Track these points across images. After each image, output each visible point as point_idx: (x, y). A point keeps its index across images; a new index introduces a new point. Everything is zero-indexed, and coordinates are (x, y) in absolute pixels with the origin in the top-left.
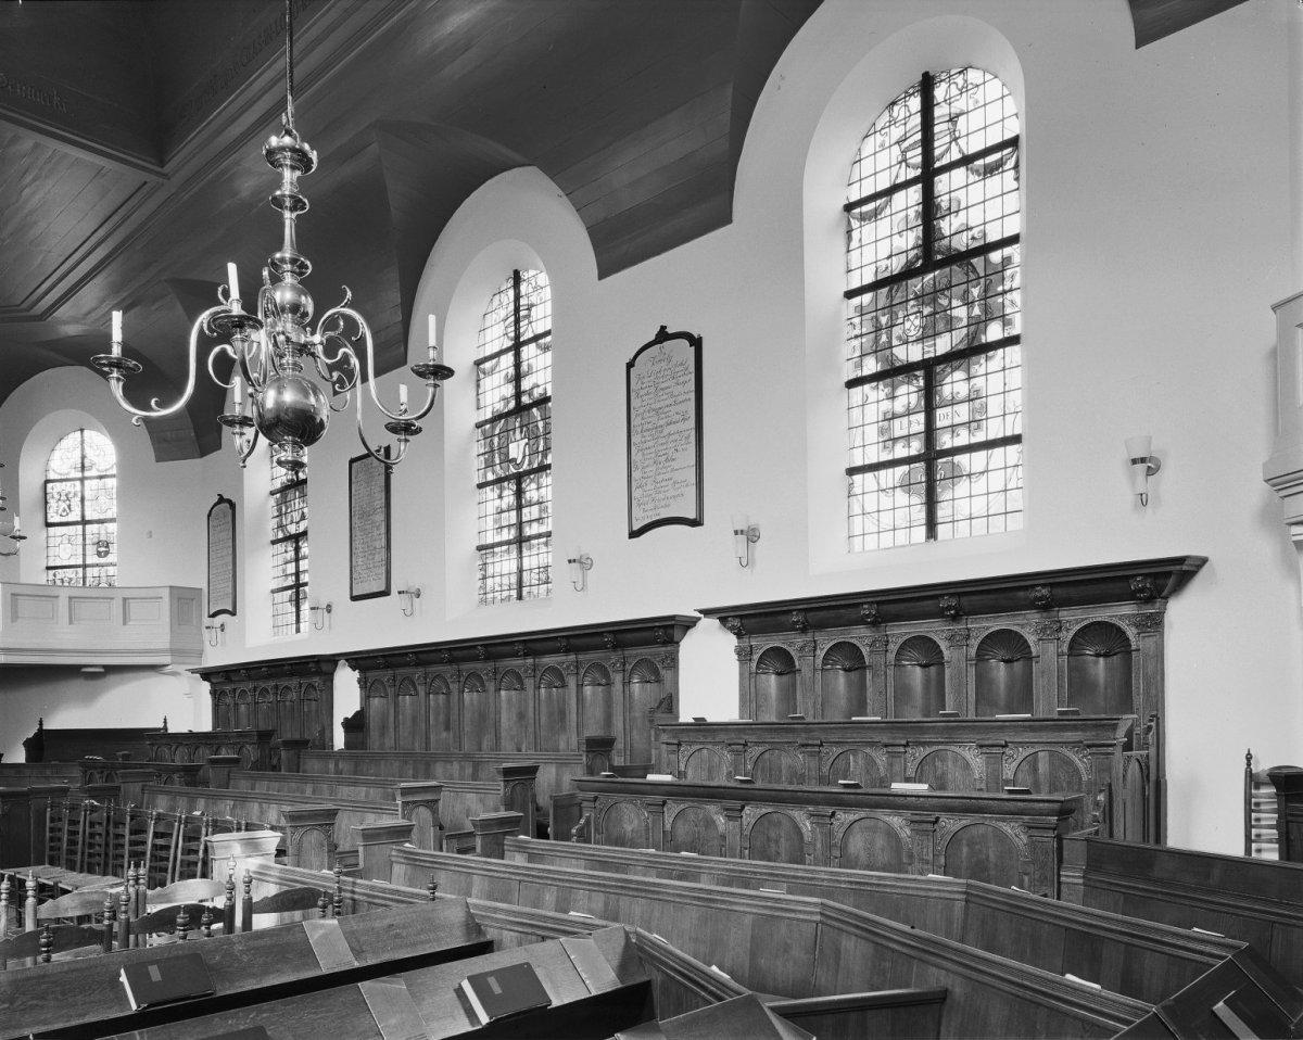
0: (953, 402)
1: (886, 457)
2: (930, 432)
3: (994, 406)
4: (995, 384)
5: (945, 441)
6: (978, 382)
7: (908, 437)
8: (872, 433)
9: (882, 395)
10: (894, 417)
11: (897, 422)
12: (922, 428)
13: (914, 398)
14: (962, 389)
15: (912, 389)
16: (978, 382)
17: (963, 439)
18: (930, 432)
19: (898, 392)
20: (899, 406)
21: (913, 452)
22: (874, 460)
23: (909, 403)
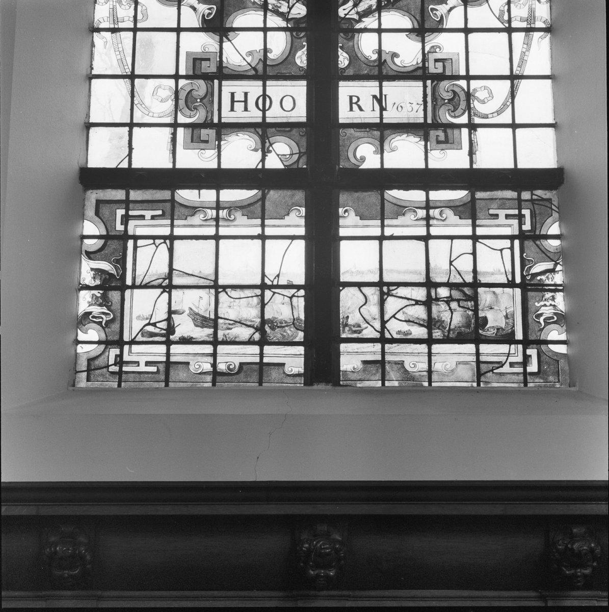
0: (381, 71)
1: (192, 159)
2: (321, 129)
3: (490, 98)
4: (489, 54)
5: (367, 155)
6: (448, 44)
7: (264, 131)
8: (157, 100)
9: (190, 19)
10: (223, 73)
11: (229, 87)
12: (300, 114)
13: (278, 44)
14: (407, 51)
15: (274, 21)
16: (448, 44)
17: (406, 153)
18: (321, 129)
19: (240, 20)
20: (240, 50)
21: (273, 163)
22: (165, 163)
23: (266, 50)
